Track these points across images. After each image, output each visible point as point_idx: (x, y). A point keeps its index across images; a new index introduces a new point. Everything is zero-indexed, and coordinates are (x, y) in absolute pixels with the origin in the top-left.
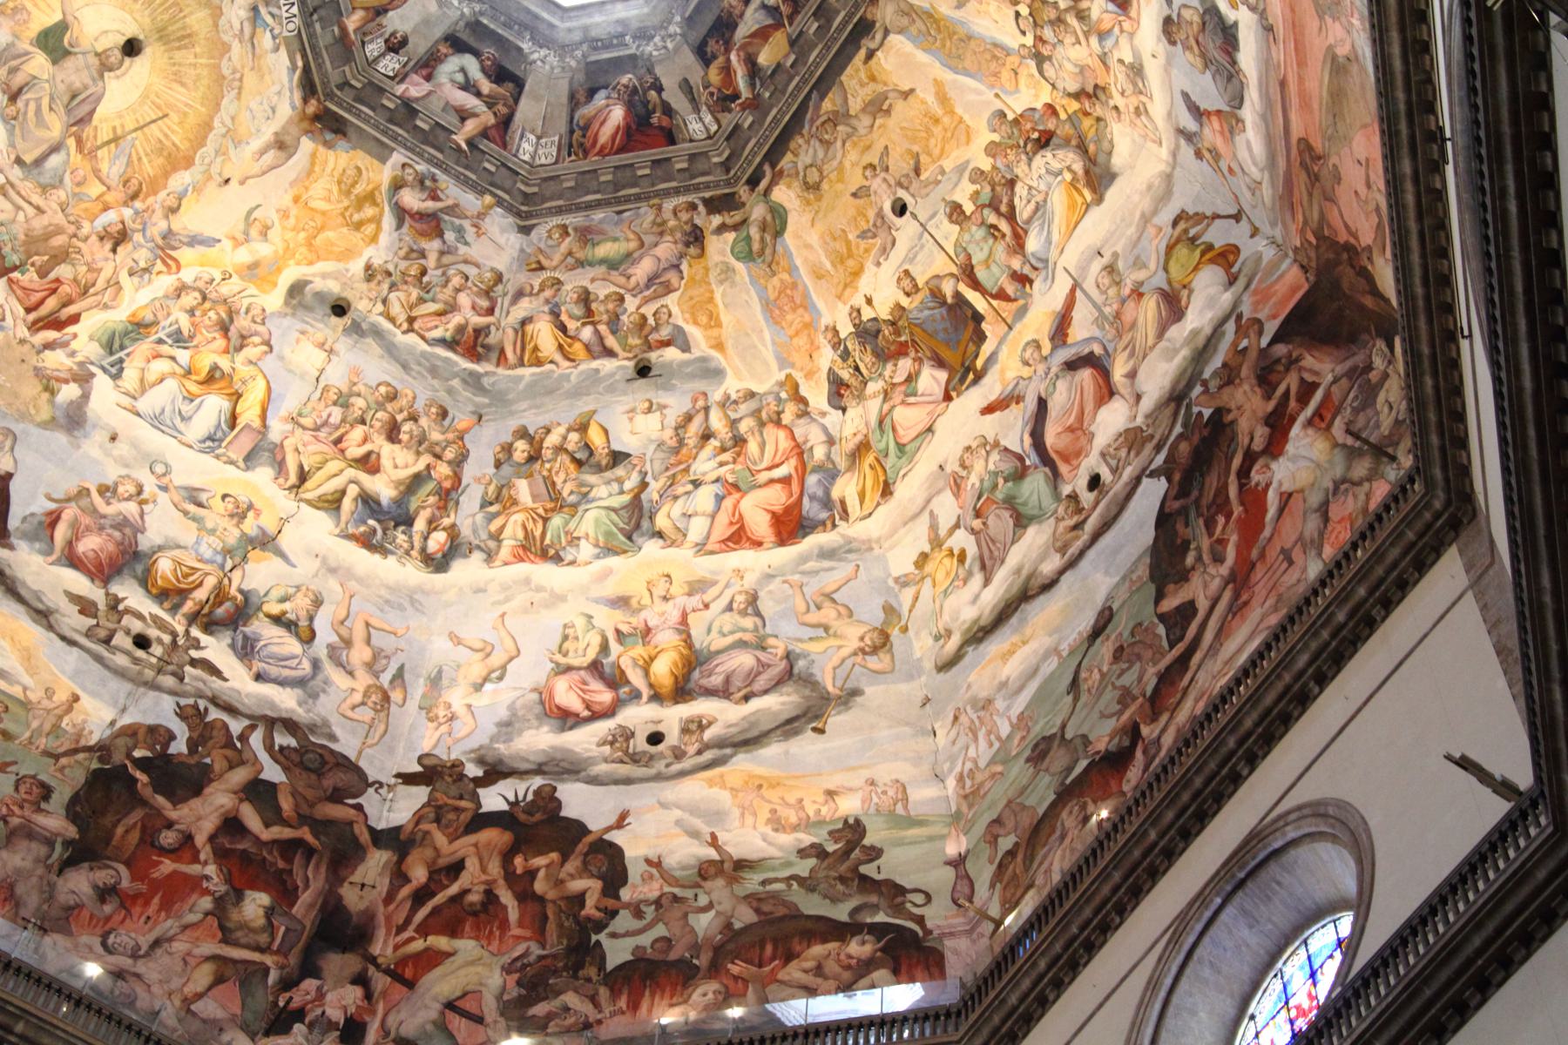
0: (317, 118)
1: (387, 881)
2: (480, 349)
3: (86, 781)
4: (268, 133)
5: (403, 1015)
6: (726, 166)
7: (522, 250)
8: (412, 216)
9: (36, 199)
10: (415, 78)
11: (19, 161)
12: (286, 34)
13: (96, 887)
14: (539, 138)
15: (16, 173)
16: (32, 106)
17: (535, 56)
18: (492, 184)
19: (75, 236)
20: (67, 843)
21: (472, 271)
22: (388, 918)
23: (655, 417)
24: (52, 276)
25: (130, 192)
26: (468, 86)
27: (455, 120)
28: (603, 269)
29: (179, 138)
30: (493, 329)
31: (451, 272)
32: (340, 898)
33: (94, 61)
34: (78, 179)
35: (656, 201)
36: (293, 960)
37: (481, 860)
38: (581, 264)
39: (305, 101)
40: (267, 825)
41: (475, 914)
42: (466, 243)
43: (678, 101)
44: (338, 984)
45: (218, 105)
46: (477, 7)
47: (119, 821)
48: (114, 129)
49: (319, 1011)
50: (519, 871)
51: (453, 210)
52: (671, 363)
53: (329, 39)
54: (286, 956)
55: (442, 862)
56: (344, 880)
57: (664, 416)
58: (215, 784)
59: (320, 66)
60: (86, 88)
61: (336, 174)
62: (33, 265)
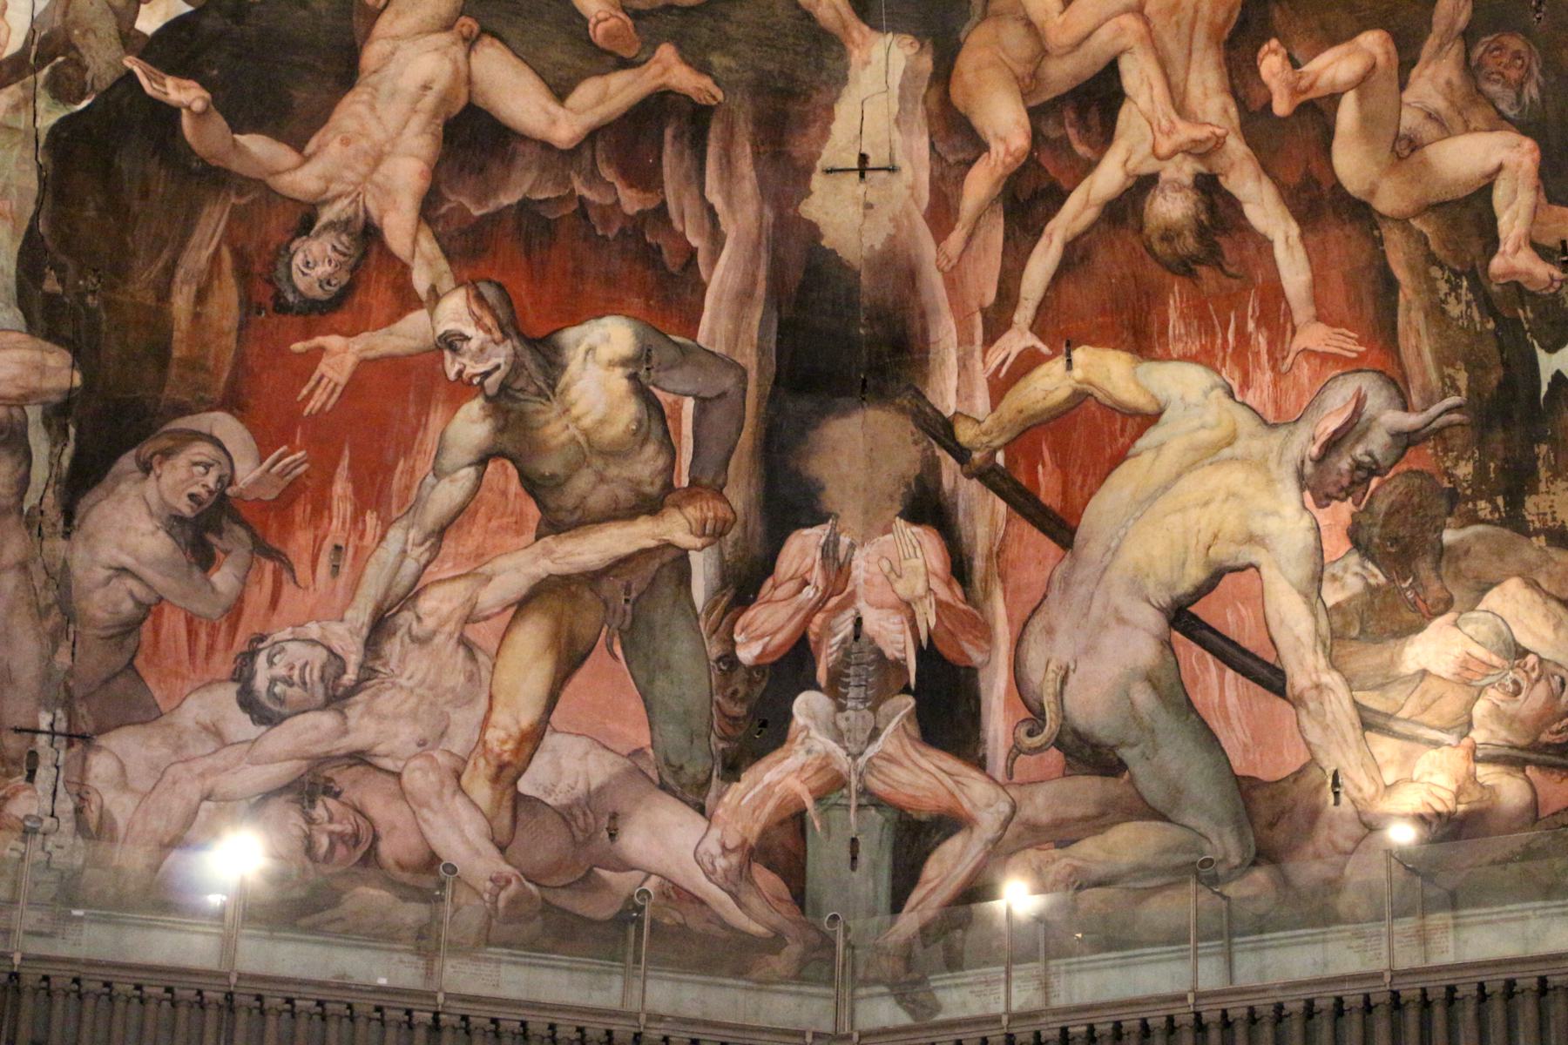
1: (922, 144)
3: (42, 181)
5: (1063, 649)
13: (174, 523)
20: (59, 413)
22: (953, 281)
32: (813, 230)
36: (740, 493)
37: (1163, 64)
40: (560, 92)
41: (1185, 268)
44: (875, 526)
47: (170, 270)
49: (845, 627)
50: (1281, 107)
54: (719, 493)
55: (1062, 73)
56: (807, 172)
58: (383, 25)
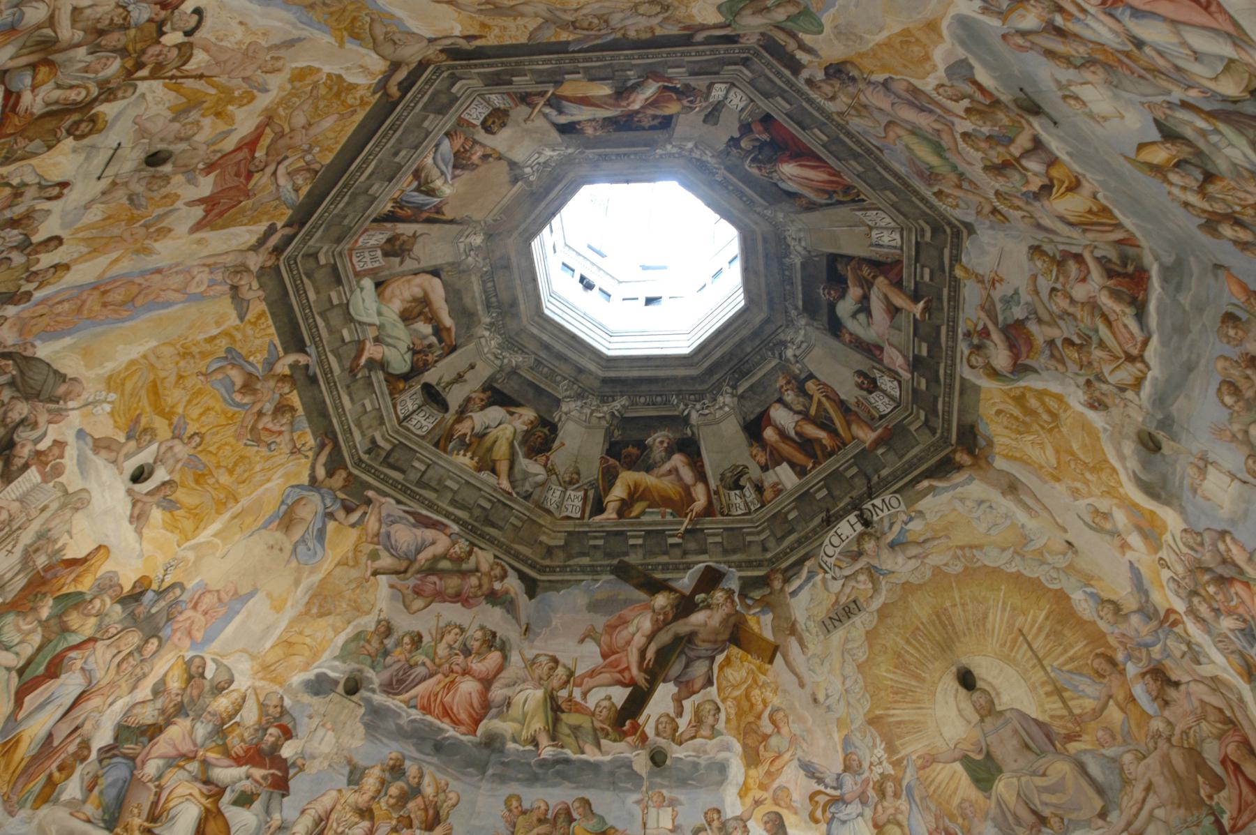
0: (971, 452)
2: (1130, 269)
4: (1006, 504)
6: (745, 62)
7: (992, 227)
8: (1016, 356)
9: (1138, 793)
10: (886, 361)
11: (1103, 815)
12: (903, 507)
14: (871, 228)
15: (1113, 816)
16: (1046, 797)
17: (799, 249)
18: (943, 270)
19: (1169, 740)
21: (1044, 284)
23: (1087, 93)
24: (1219, 770)
25: (1107, 667)
26: (864, 307)
27: (902, 318)
28: (948, 155)
29: (1040, 612)
30: (1098, 253)
31: (1054, 308)
33: (988, 720)
34: (1107, 737)
35: (836, 117)
38: (961, 176)
39: (960, 467)
42: (1016, 292)
43: (728, 127)
45: (996, 571)
46: (793, 313)
48: (1048, 694)
51: (989, 309)
52: (995, 78)
53: (891, 457)
57: (1070, 83)
59: (920, 459)
60: (1016, 732)
61: (1014, 436)
62: (1211, 797)
